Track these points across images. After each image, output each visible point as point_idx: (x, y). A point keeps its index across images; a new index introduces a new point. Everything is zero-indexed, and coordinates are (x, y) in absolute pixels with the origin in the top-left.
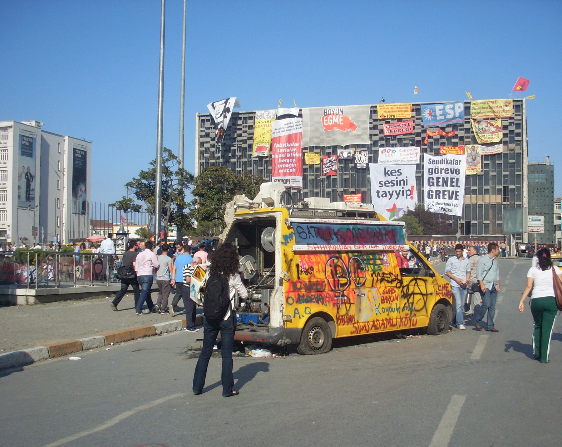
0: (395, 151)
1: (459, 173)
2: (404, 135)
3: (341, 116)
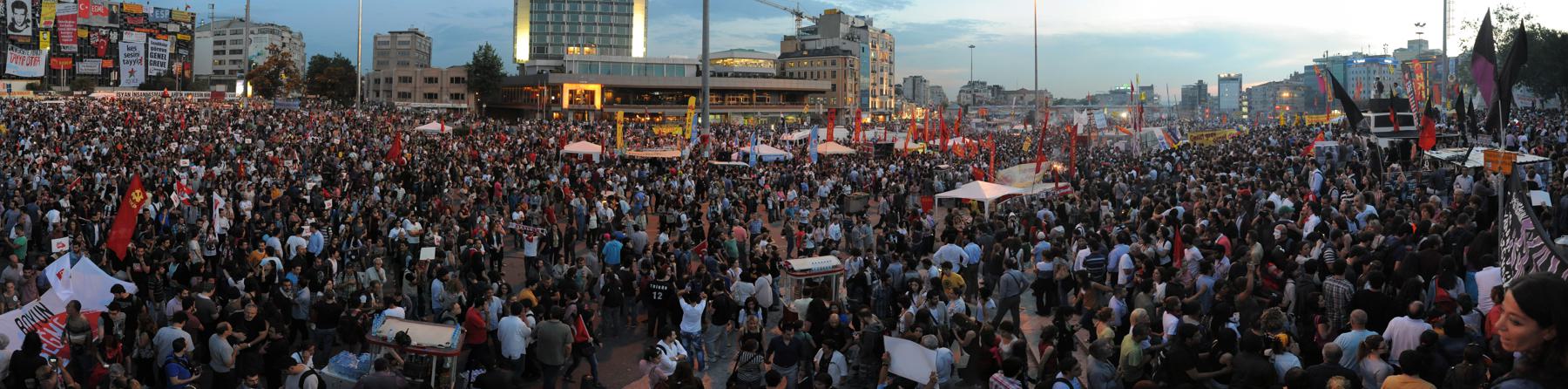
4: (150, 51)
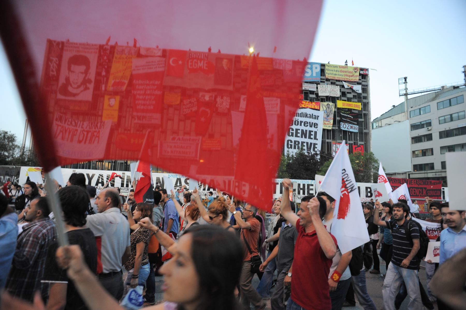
1: (317, 127)
3: (205, 62)
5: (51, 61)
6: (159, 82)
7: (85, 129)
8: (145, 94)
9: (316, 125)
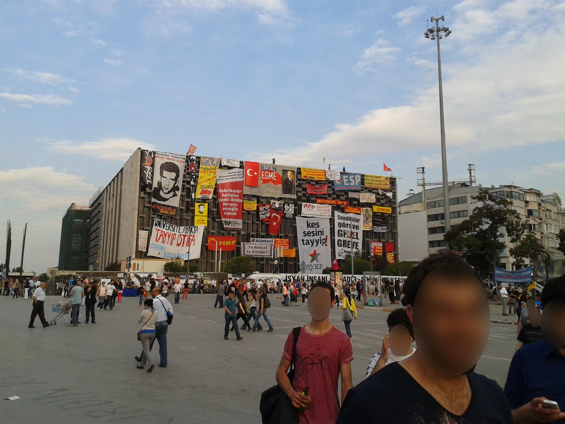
0: (314, 207)
1: (358, 229)
2: (322, 194)
3: (274, 173)
4: (337, 228)
5: (146, 169)
6: (241, 191)
7: (182, 234)
8: (230, 202)
9: (357, 227)
